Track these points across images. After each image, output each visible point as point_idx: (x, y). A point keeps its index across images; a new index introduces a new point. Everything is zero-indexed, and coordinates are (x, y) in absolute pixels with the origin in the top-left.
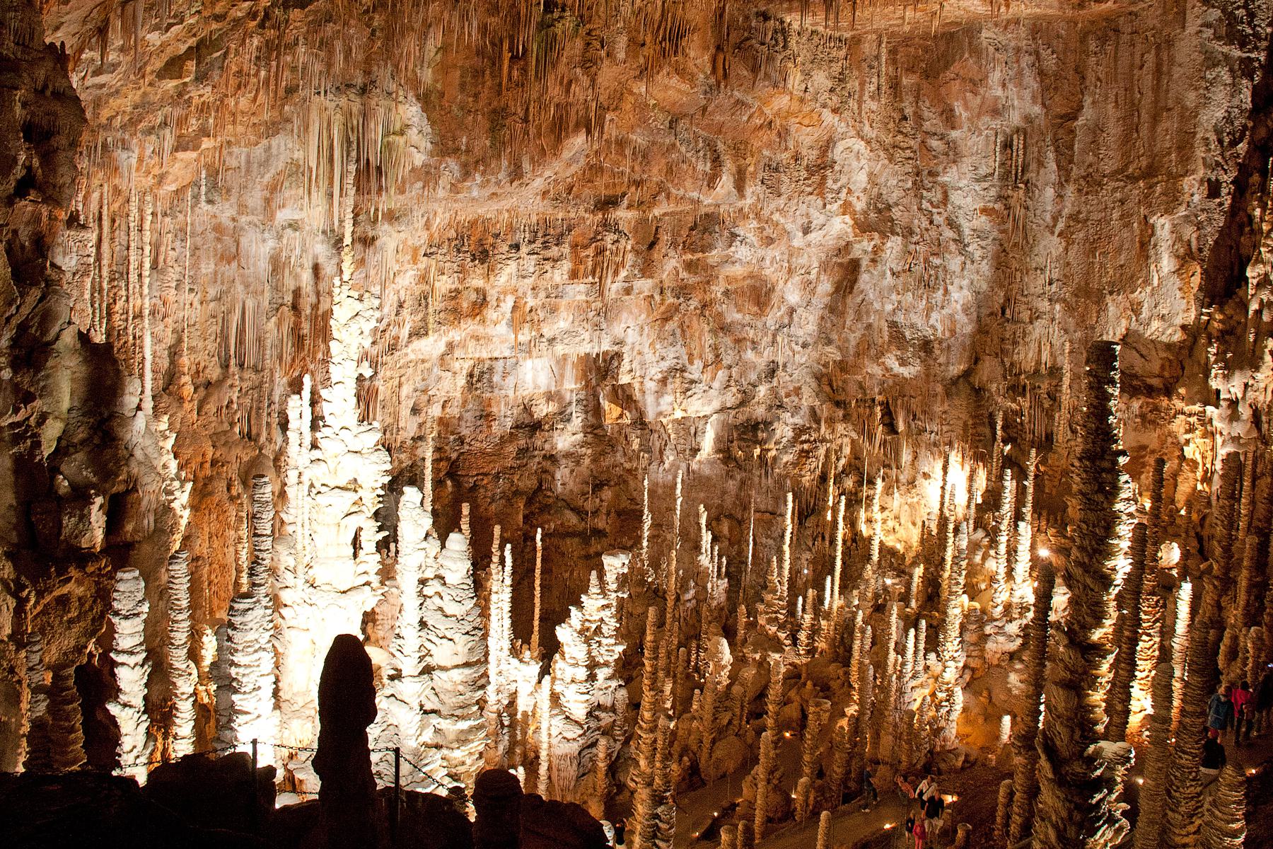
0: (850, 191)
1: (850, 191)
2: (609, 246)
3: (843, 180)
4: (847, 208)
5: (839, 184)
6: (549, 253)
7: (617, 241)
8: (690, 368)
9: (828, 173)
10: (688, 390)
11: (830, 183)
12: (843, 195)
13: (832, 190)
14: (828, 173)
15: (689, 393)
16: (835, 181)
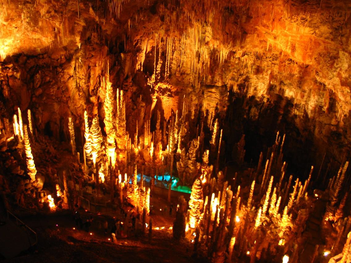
0: (341, 70)
1: (341, 70)
2: (287, 65)
3: (340, 65)
4: (339, 75)
5: (338, 66)
6: (273, 62)
7: (290, 64)
8: (324, 107)
9: (336, 61)
10: (321, 114)
11: (335, 65)
12: (338, 70)
13: (335, 67)
14: (336, 61)
15: (321, 115)
16: (337, 64)
